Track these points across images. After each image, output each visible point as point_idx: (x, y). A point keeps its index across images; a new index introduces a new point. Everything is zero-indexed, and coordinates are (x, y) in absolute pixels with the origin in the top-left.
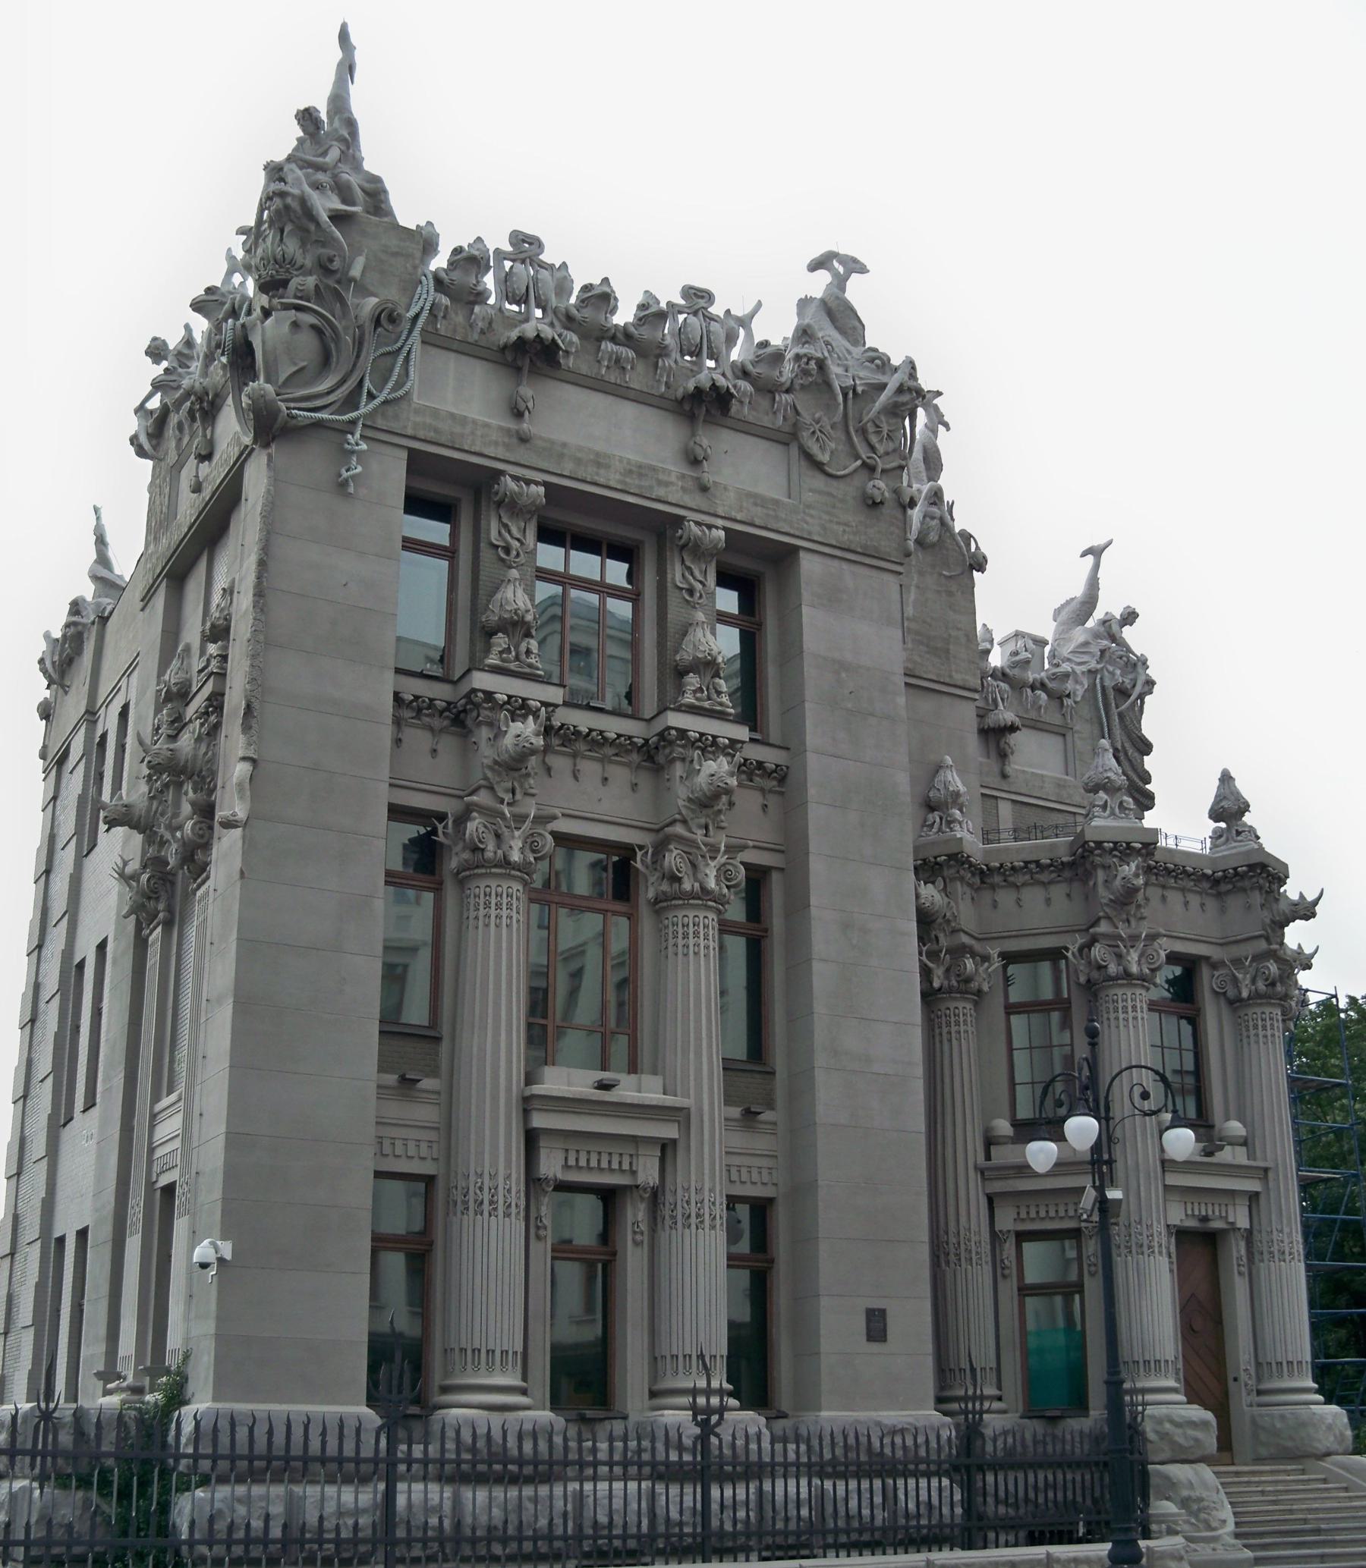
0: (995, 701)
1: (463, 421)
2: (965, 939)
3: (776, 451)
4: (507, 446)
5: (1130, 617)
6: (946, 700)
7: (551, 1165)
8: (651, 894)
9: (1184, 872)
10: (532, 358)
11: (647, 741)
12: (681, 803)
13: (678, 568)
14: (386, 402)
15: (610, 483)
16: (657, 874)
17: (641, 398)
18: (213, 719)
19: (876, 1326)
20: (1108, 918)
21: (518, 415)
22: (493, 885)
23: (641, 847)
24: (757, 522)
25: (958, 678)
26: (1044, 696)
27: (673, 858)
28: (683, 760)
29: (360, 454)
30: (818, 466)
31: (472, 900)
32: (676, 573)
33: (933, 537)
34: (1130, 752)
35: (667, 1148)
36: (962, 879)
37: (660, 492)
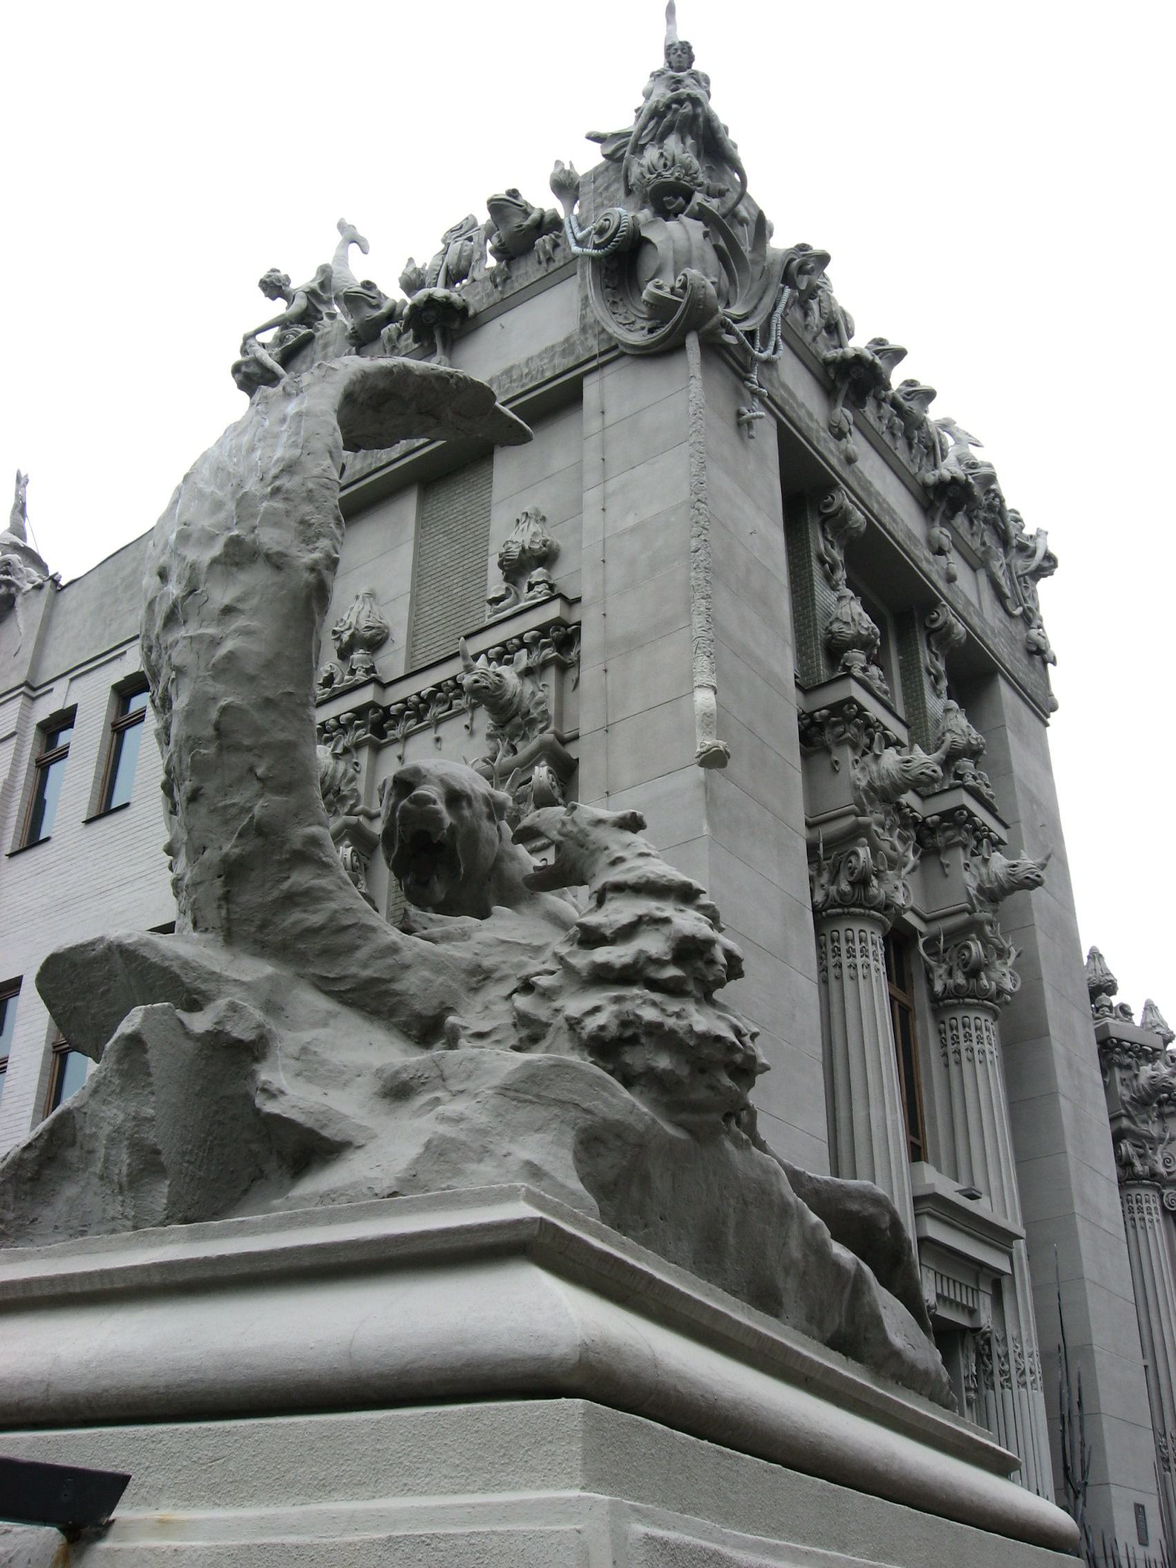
1: (810, 415)
8: (938, 987)
11: (924, 819)
12: (973, 892)
13: (927, 652)
16: (945, 966)
18: (550, 653)
20: (1129, 1117)
22: (868, 930)
23: (921, 934)
24: (979, 631)
27: (976, 948)
28: (965, 847)
31: (844, 946)
32: (925, 657)
35: (997, 1283)
37: (924, 566)
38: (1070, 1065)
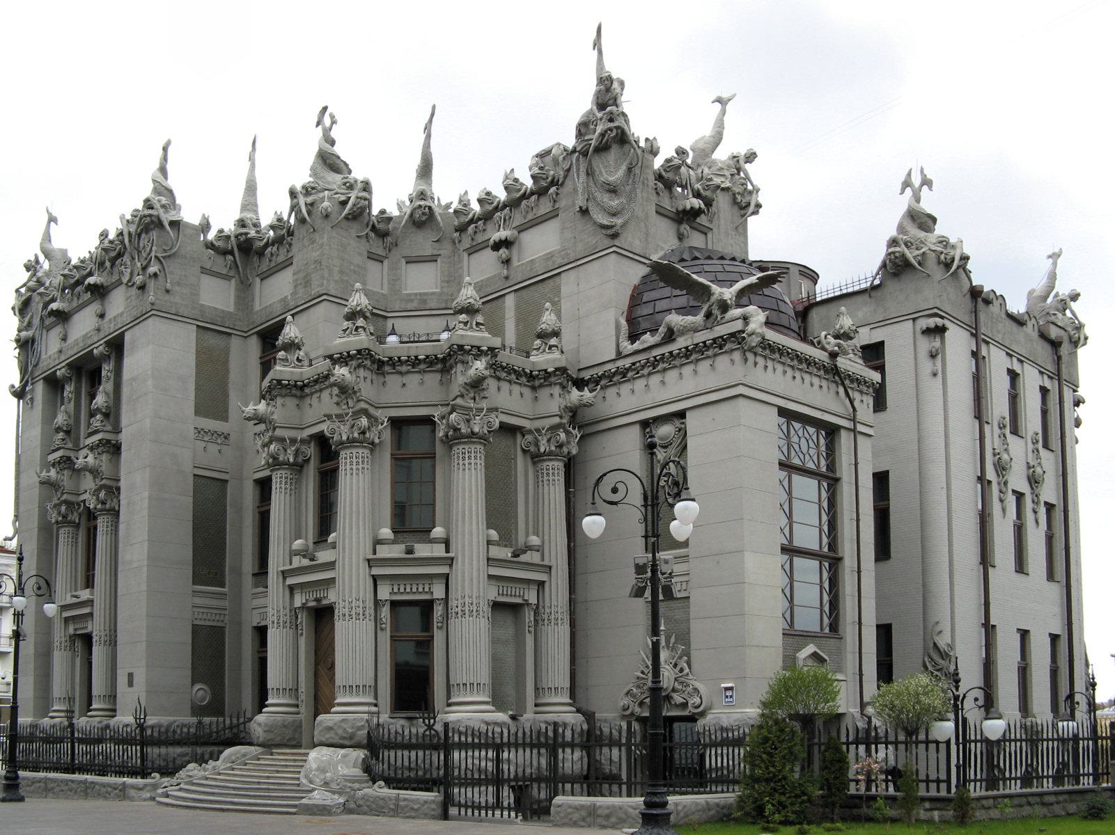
6: (312, 309)
25: (316, 290)
37: (89, 342)
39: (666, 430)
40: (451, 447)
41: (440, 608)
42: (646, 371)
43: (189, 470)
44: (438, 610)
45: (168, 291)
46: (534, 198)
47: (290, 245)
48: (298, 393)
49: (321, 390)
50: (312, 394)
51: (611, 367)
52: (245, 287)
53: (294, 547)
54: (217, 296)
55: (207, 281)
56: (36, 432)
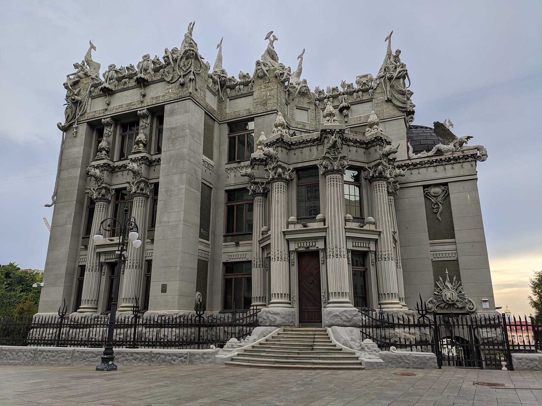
0: (342, 101)
1: (95, 112)
2: (256, 180)
3: (163, 83)
4: (104, 113)
5: (398, 52)
7: (102, 259)
9: (307, 141)
10: (107, 92)
14: (81, 115)
15: (124, 110)
17: (133, 88)
19: (164, 289)
21: (108, 105)
26: (360, 93)
29: (76, 128)
30: (169, 82)
33: (261, 74)
34: (396, 96)
36: (256, 164)
37: (133, 107)
38: (167, 191)
39: (438, 190)
40: (371, 183)
41: (374, 255)
42: (427, 165)
43: (200, 178)
44: (371, 257)
45: (196, 90)
46: (360, 93)
47: (252, 86)
48: (288, 148)
49: (303, 148)
50: (296, 149)
51: (410, 162)
52: (220, 101)
53: (289, 220)
54: (211, 101)
55: (208, 93)
56: (78, 149)
